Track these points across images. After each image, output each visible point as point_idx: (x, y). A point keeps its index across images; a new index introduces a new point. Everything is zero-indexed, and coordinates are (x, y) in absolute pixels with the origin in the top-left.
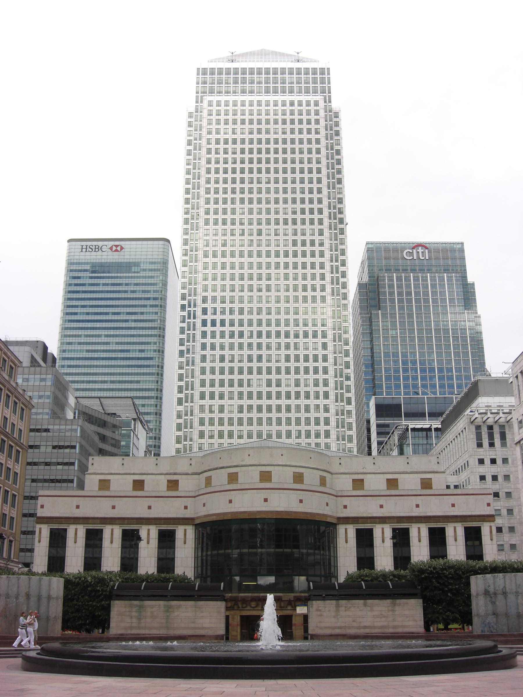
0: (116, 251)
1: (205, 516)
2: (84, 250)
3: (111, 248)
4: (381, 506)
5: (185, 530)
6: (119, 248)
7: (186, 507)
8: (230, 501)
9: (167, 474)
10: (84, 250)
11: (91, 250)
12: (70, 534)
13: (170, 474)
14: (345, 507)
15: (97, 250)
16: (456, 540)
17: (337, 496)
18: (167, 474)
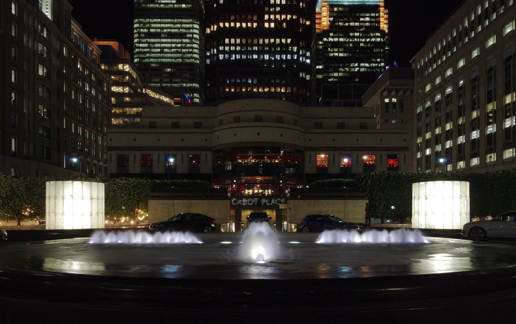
4: (334, 140)
5: (206, 155)
7: (206, 140)
8: (235, 135)
9: (194, 118)
12: (131, 158)
13: (196, 118)
14: (310, 140)
16: (381, 163)
17: (305, 133)
18: (194, 118)
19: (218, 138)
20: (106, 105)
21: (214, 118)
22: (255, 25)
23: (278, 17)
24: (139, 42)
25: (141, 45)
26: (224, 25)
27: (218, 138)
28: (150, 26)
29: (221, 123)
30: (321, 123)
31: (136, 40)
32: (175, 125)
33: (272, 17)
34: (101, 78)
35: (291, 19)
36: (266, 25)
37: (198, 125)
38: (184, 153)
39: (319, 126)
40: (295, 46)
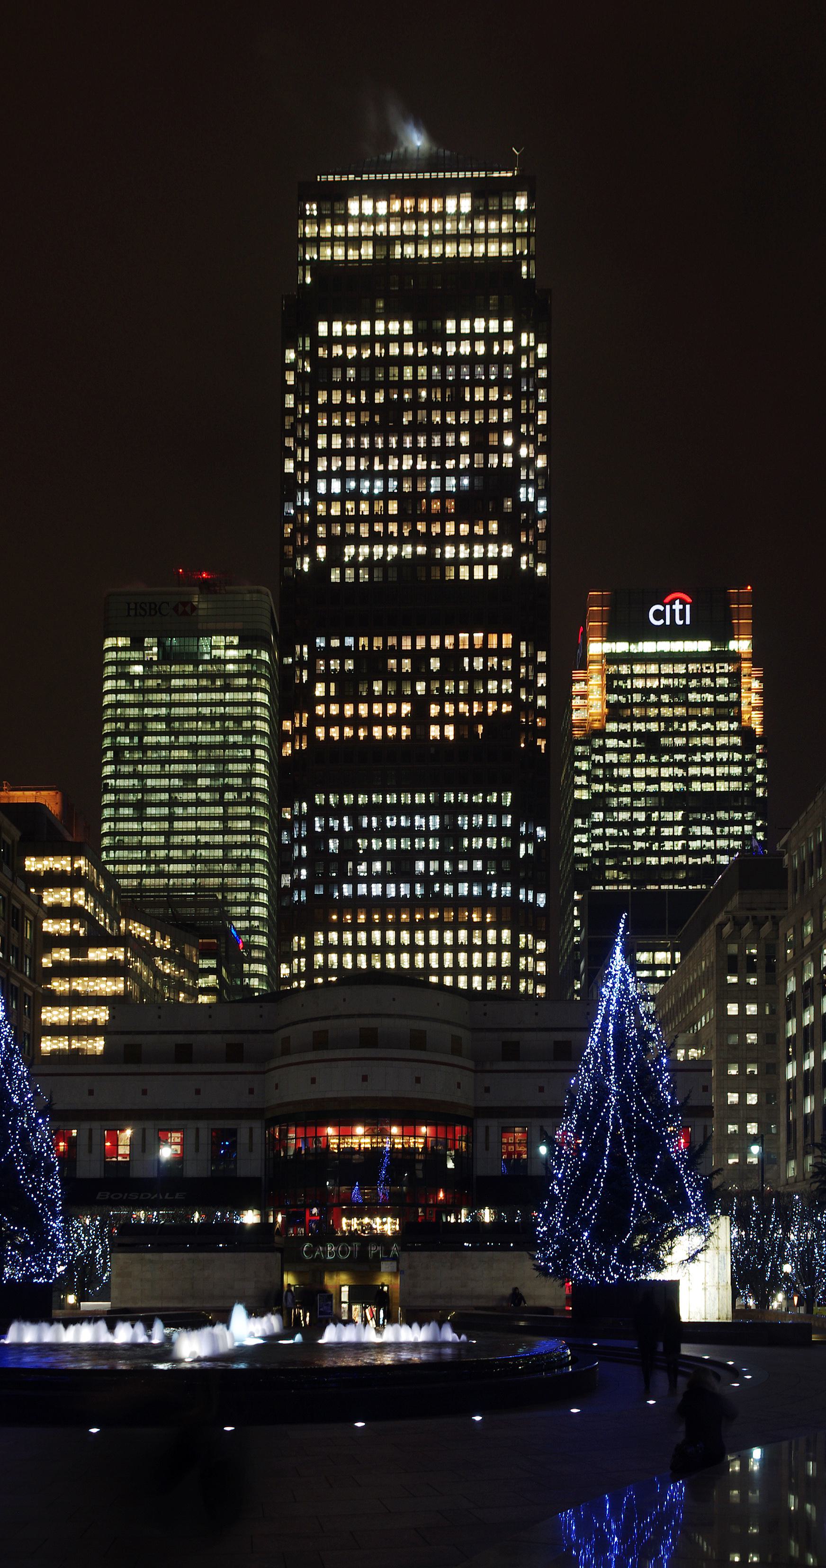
0: (185, 613)
1: (280, 1105)
2: (132, 613)
3: (176, 609)
6: (188, 609)
7: (251, 1091)
10: (132, 613)
11: (143, 613)
14: (487, 1090)
15: (153, 612)
17: (475, 1071)
19: (277, 1087)
20: (28, 981)
21: (272, 1032)
22: (405, 732)
23: (463, 707)
24: (116, 775)
25: (120, 783)
26: (327, 732)
27: (277, 1087)
28: (144, 727)
29: (286, 1051)
30: (518, 1043)
31: (108, 770)
32: (184, 1054)
33: (449, 709)
34: (18, 906)
35: (498, 712)
36: (434, 731)
37: (235, 1054)
38: (202, 1125)
39: (511, 1052)
40: (506, 791)
